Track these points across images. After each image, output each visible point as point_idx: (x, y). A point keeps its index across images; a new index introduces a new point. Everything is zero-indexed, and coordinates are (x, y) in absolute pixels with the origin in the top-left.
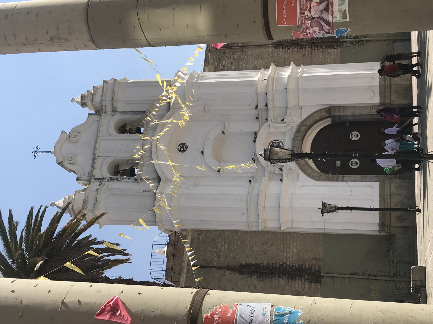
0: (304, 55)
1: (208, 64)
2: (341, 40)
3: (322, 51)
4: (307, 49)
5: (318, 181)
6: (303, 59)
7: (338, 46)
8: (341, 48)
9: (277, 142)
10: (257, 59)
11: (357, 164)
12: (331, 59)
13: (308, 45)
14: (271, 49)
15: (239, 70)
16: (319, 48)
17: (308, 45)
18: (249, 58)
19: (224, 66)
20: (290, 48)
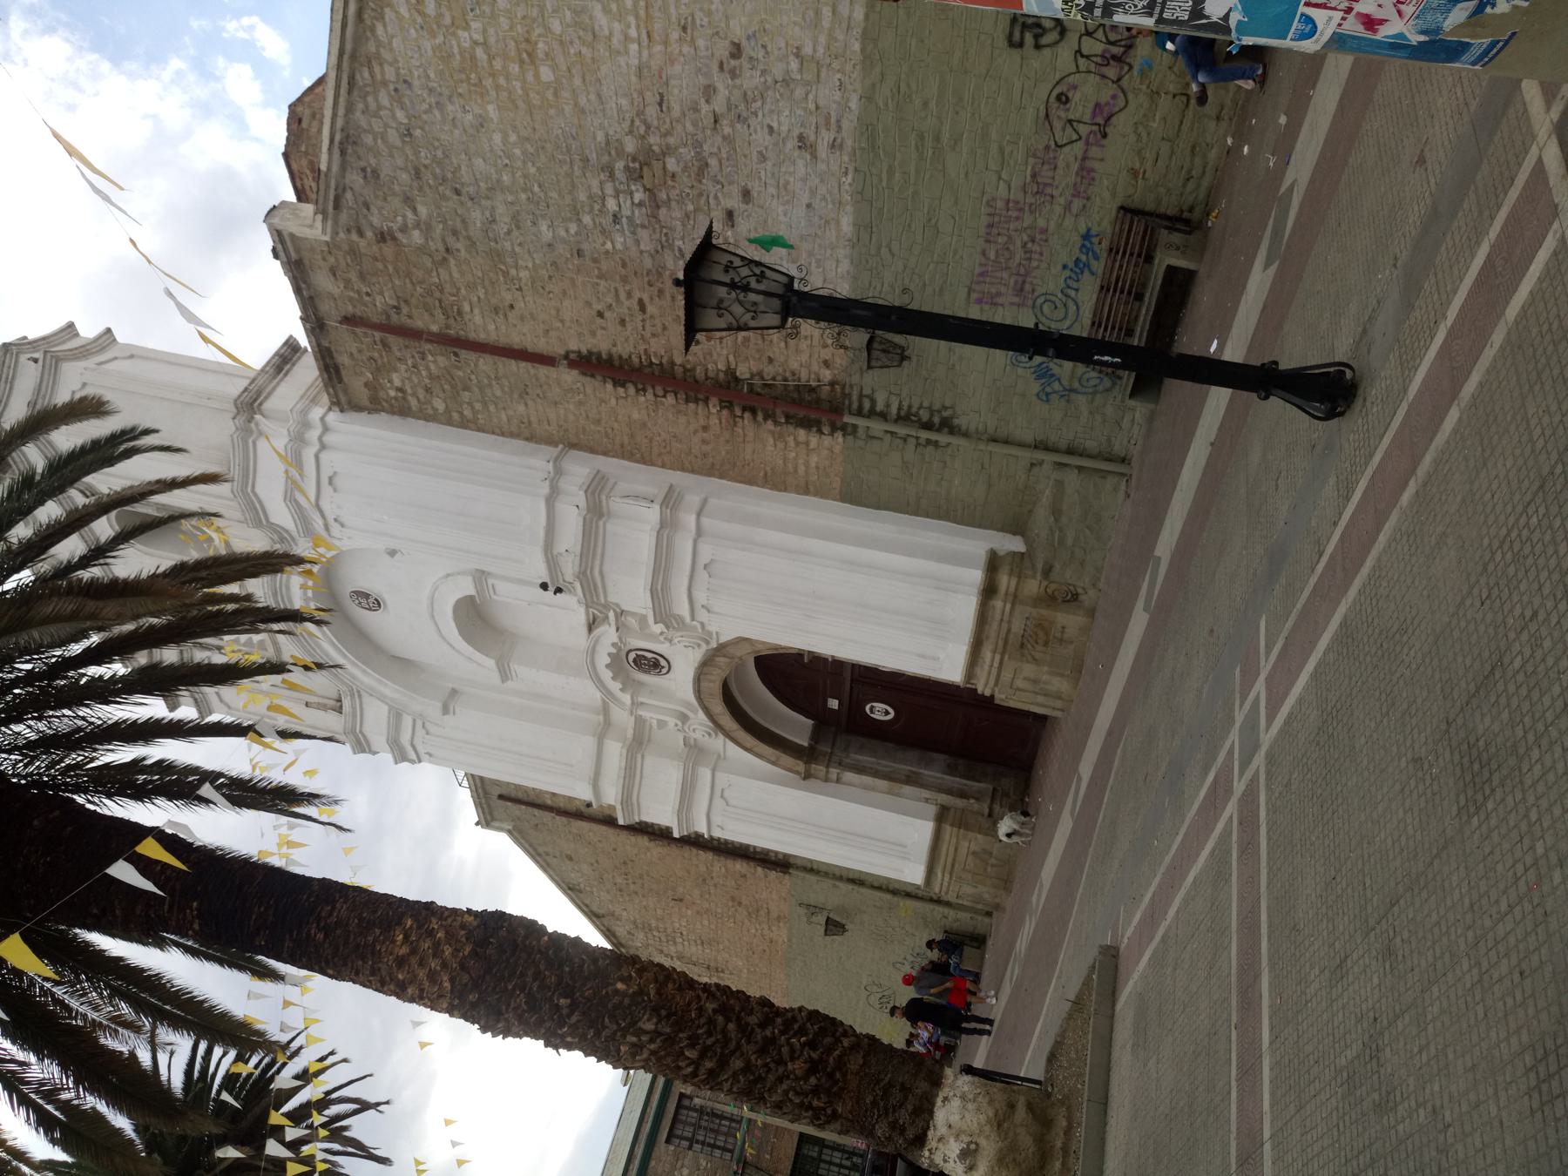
0: (705, 428)
1: (338, 371)
2: (848, 419)
3: (773, 433)
4: (714, 410)
5: (773, 763)
6: (704, 442)
7: (834, 429)
8: (850, 438)
9: (649, 655)
10: (521, 396)
11: (887, 713)
12: (807, 464)
13: (714, 401)
14: (570, 377)
15: (464, 424)
16: (760, 417)
17: (714, 401)
18: (490, 385)
19: (400, 390)
20: (644, 390)
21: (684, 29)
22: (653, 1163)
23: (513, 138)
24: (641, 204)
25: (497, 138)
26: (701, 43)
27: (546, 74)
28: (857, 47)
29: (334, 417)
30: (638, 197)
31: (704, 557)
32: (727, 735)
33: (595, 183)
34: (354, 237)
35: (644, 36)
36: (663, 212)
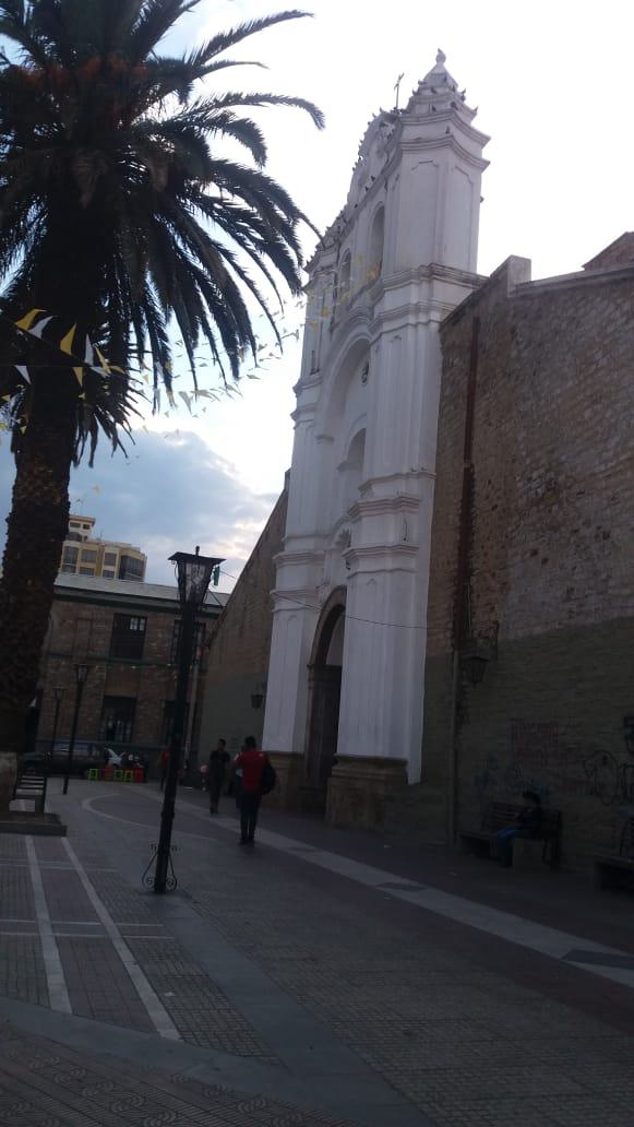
21: (613, 499)
22: (162, 614)
23: (559, 401)
24: (536, 492)
25: (558, 391)
26: (608, 511)
27: (587, 414)
28: (615, 615)
29: (434, 326)
30: (539, 490)
31: (379, 578)
32: (323, 610)
33: (543, 462)
34: (512, 313)
35: (609, 473)
36: (535, 508)
